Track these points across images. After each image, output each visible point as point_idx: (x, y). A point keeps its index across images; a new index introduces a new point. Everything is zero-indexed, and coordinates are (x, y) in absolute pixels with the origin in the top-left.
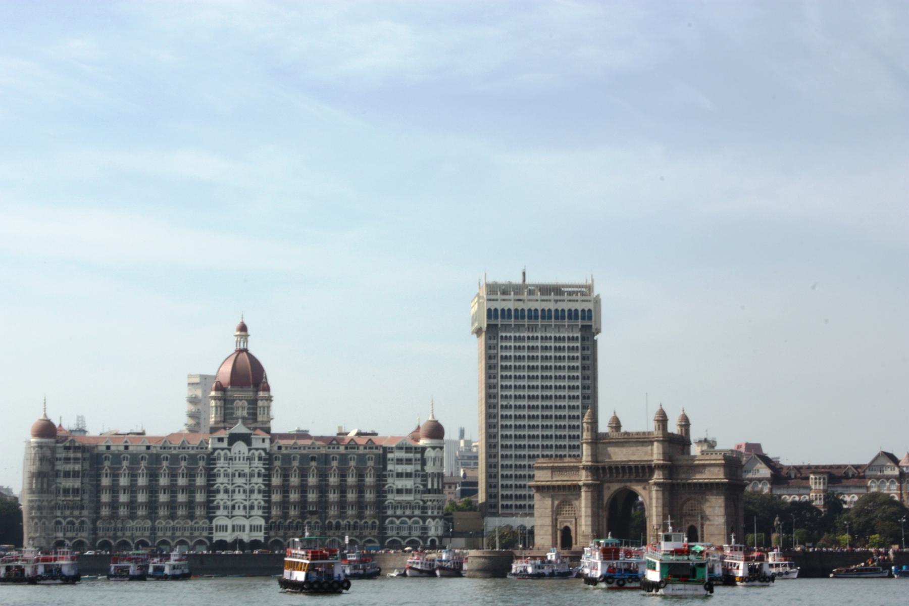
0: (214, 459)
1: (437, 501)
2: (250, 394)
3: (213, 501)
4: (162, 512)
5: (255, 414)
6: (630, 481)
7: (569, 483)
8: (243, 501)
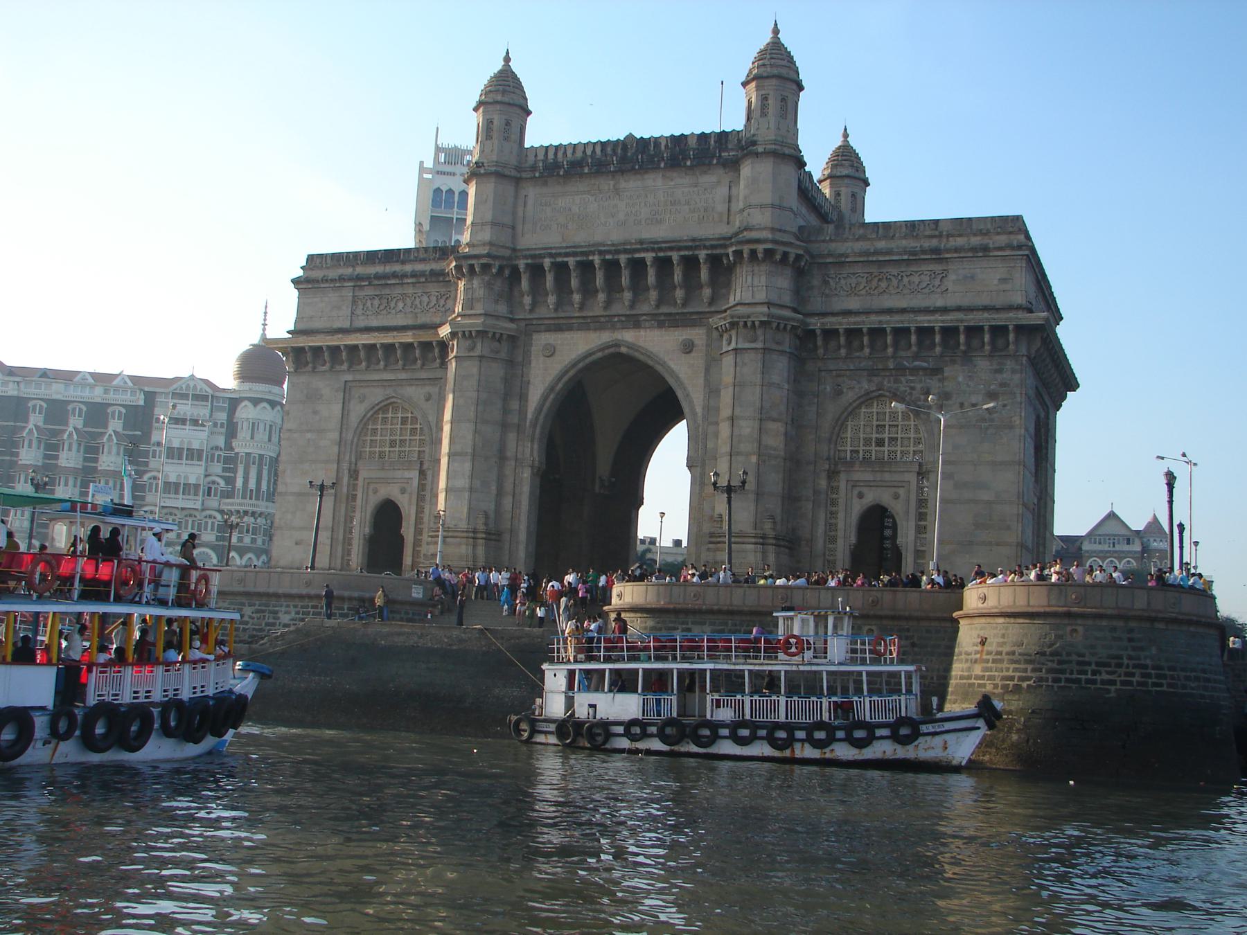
1: (253, 514)
6: (634, 322)
7: (408, 338)
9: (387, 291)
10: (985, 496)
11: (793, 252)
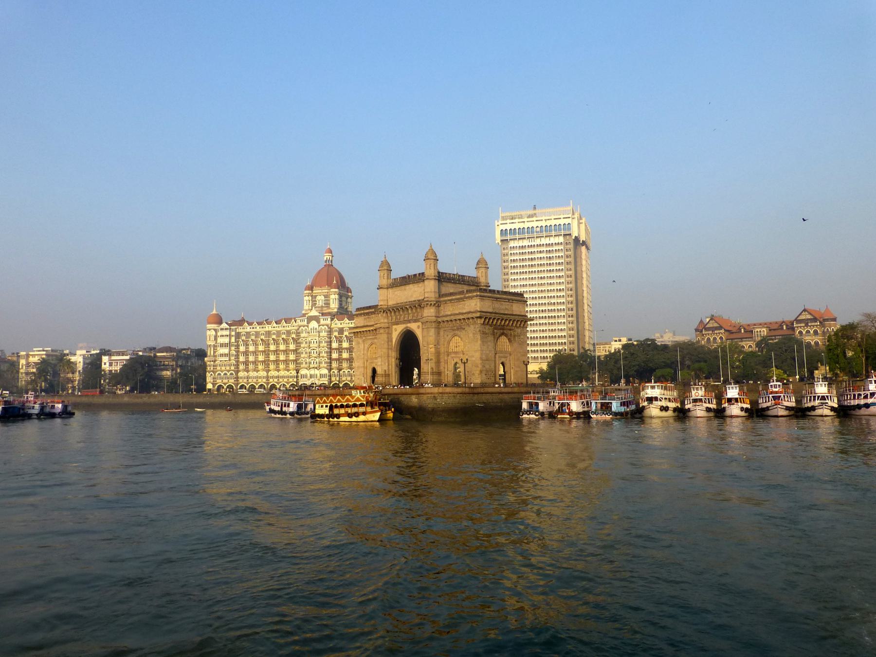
0: (299, 333)
2: (326, 291)
3: (299, 359)
4: (272, 367)
5: (329, 304)
6: (409, 321)
7: (372, 328)
8: (316, 359)
9: (370, 316)
10: (474, 359)
11: (433, 303)
